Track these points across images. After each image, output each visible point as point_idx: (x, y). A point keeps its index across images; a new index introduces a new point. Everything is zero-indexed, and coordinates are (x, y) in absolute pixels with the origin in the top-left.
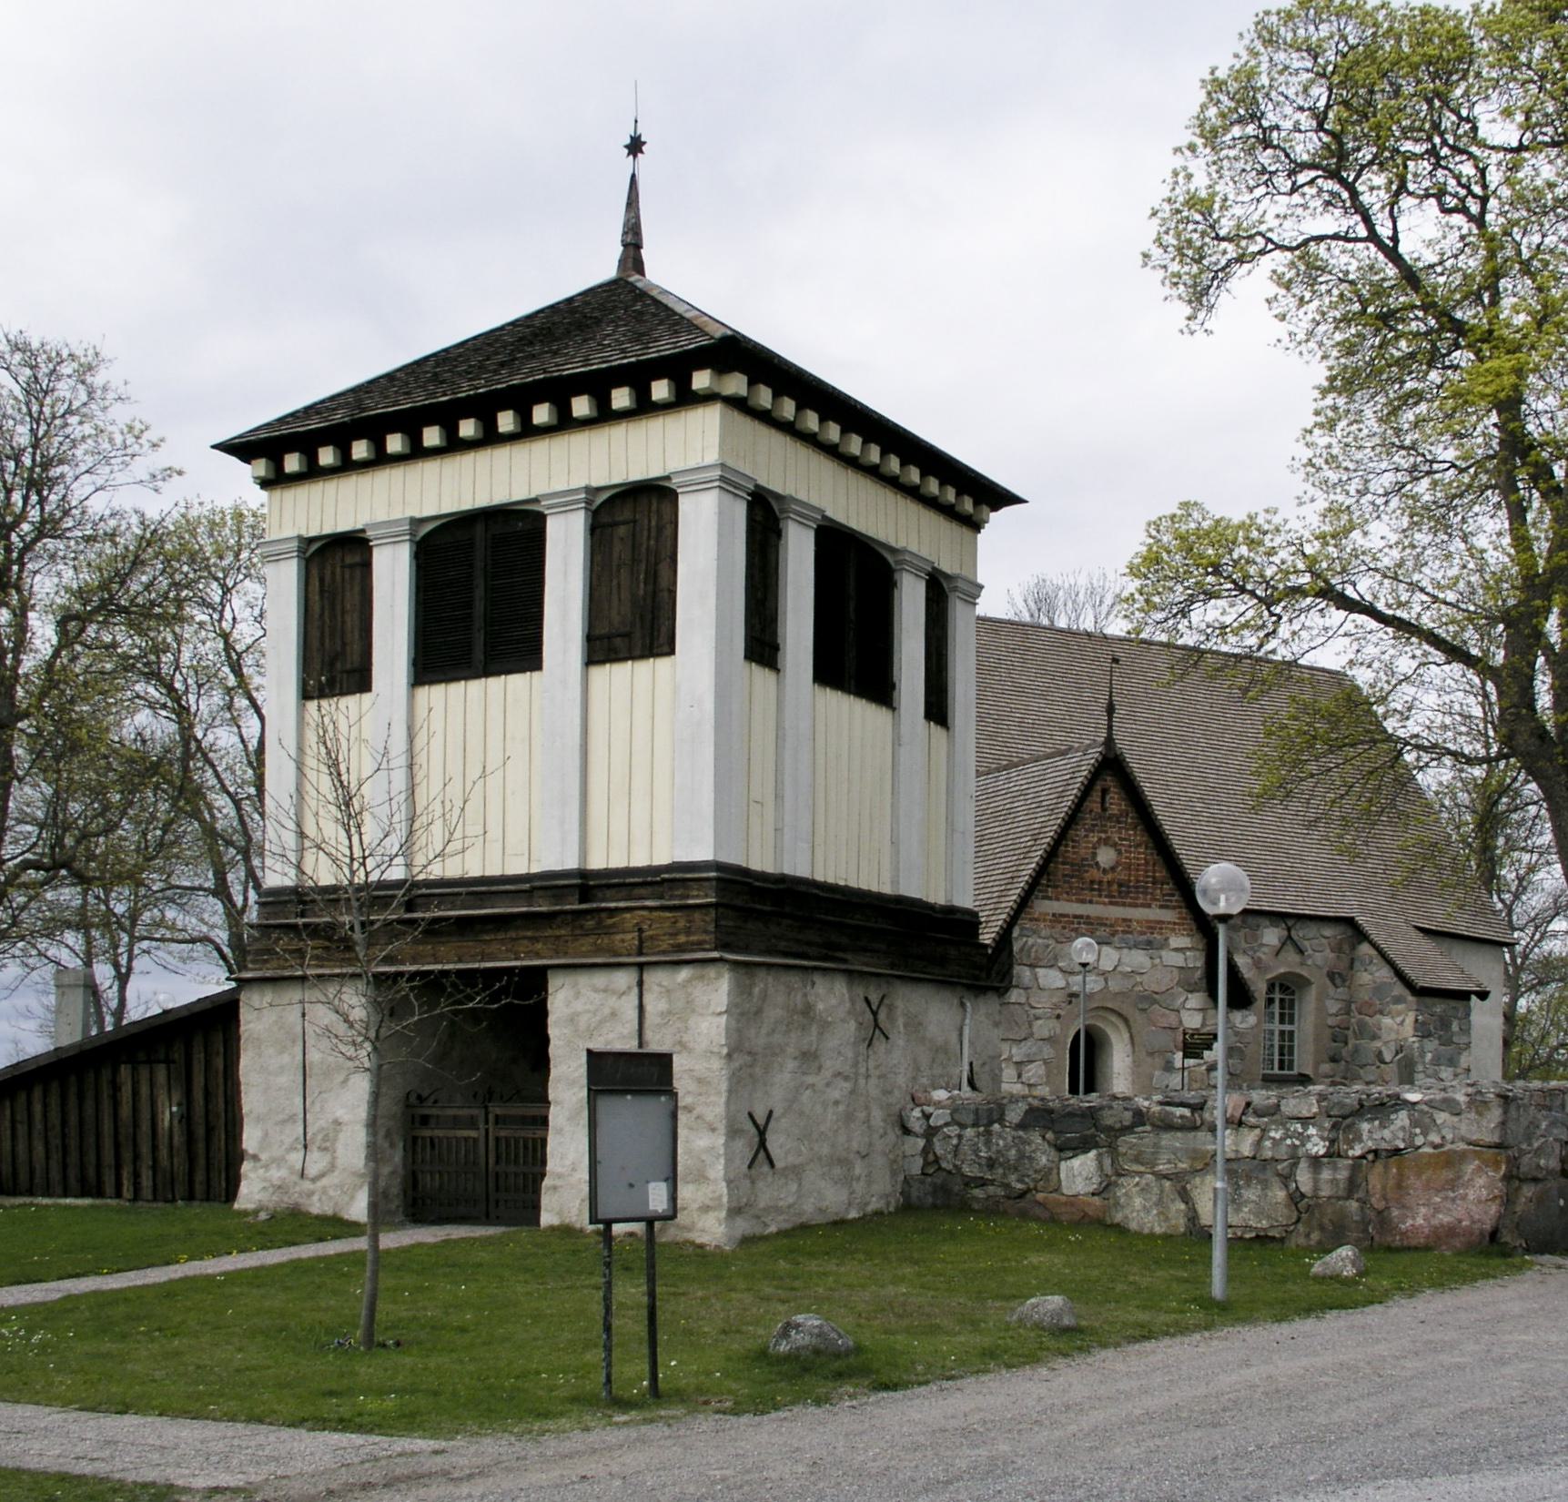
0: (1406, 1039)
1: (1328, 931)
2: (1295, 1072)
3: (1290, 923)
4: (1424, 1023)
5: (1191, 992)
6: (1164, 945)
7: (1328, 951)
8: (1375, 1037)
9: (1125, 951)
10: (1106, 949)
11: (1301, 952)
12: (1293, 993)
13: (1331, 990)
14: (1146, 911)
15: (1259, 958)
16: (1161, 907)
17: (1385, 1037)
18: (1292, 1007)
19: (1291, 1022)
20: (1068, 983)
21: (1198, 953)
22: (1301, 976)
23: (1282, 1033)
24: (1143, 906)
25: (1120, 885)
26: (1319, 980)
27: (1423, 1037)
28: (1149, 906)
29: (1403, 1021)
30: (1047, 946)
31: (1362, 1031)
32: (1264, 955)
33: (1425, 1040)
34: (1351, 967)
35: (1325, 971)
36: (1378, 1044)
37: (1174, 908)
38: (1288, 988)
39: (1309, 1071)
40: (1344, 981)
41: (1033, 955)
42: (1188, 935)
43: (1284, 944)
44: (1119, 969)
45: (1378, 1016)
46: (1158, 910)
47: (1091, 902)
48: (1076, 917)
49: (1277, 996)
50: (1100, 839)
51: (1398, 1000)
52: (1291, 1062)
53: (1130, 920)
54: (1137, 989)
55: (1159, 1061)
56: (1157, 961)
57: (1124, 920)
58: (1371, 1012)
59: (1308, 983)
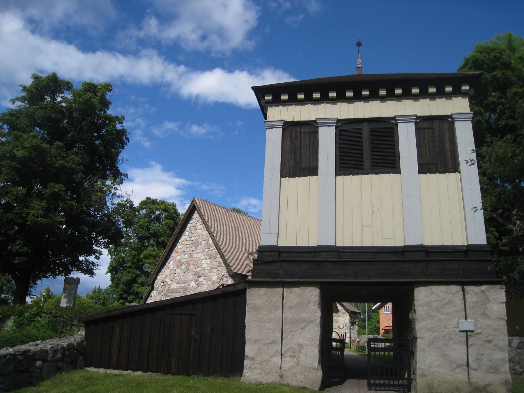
0: (347, 323)
17: (340, 322)
36: (338, 324)
51: (344, 313)
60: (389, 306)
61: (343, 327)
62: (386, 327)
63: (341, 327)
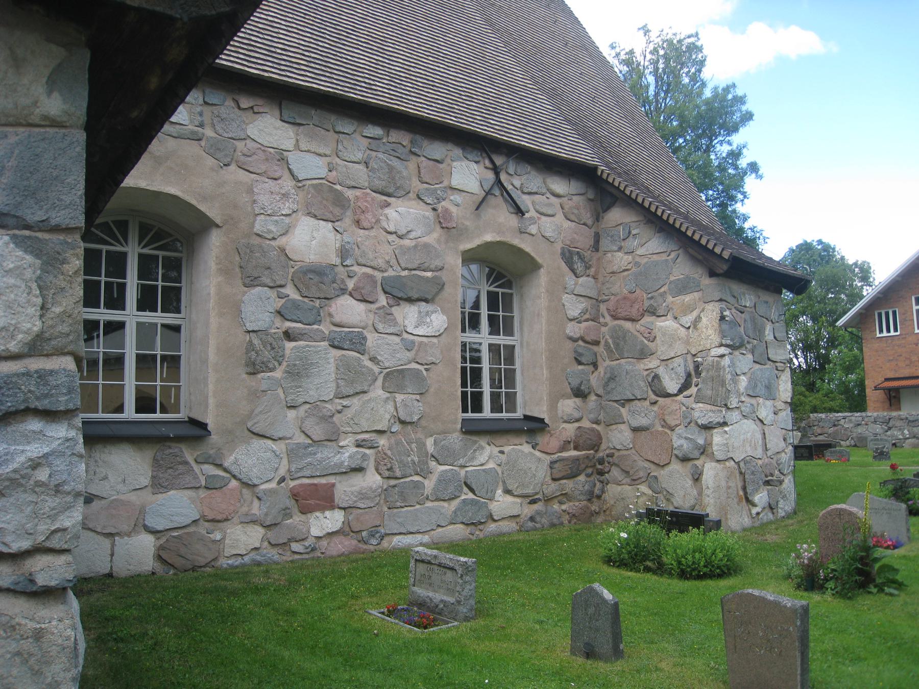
1: (559, 185)
2: (519, 414)
3: (499, 160)
4: (734, 324)
7: (560, 217)
8: (643, 354)
11: (519, 211)
12: (509, 284)
13: (570, 279)
15: (446, 210)
17: (663, 351)
18: (508, 307)
19: (509, 332)
23: (494, 349)
29: (698, 319)
32: (455, 206)
33: (737, 353)
34: (596, 247)
35: (558, 247)
36: (652, 363)
40: (588, 267)
43: (488, 193)
45: (648, 319)
51: (682, 288)
52: (511, 398)
58: (634, 313)
59: (533, 266)
60: (894, 313)
61: (685, 386)
62: (887, 380)
63: (672, 386)
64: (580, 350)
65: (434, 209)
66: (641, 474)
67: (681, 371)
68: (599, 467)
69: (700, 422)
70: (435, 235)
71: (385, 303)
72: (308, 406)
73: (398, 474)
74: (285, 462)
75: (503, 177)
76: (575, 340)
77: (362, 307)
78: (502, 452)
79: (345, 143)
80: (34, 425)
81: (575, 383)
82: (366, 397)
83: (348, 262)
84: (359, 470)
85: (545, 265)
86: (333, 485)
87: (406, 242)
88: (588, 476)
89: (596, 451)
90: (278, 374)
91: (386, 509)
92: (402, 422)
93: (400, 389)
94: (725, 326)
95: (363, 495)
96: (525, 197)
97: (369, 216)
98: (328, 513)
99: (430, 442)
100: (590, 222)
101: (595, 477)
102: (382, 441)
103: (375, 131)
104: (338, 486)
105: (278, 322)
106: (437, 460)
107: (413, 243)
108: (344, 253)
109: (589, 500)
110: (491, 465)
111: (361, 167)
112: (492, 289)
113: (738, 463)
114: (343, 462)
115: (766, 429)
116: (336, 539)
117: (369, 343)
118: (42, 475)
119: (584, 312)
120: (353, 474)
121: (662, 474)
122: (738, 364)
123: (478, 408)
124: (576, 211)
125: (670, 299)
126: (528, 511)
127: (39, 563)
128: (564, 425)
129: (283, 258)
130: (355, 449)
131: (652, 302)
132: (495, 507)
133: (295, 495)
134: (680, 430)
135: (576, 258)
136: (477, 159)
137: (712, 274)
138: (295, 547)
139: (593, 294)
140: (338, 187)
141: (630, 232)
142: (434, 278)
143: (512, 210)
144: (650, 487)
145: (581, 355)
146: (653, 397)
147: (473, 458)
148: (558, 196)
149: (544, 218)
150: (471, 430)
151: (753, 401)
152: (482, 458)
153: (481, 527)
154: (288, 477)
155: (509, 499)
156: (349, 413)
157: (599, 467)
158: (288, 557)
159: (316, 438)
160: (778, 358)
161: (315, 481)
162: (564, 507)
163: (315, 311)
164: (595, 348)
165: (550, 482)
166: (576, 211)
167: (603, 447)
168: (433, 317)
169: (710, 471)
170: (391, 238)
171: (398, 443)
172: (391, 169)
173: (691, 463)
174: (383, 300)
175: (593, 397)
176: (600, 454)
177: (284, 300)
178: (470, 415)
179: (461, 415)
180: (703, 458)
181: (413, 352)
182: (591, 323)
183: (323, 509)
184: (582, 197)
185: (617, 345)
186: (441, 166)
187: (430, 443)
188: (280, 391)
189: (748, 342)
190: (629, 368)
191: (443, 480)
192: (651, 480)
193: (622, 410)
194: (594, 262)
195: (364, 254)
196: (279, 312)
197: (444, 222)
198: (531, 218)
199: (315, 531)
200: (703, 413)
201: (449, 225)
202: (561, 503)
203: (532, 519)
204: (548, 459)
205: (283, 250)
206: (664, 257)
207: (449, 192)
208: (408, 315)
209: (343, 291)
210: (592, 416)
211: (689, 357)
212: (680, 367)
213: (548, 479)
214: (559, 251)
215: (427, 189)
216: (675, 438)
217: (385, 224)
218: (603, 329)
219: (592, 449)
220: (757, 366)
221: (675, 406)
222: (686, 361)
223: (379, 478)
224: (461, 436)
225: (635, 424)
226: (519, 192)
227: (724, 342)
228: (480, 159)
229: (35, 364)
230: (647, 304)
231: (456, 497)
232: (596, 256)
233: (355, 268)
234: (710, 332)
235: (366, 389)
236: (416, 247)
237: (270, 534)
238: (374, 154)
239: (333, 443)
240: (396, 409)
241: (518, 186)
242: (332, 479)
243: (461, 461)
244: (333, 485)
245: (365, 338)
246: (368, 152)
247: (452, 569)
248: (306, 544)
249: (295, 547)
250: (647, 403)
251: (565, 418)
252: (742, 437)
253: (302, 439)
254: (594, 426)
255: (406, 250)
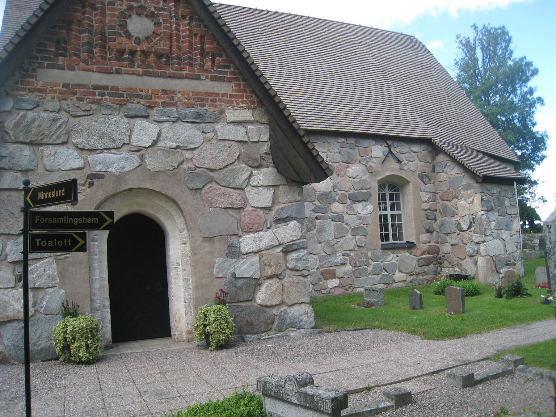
3: (390, 143)
4: (487, 201)
5: (257, 167)
6: (218, 118)
7: (417, 161)
8: (454, 214)
9: (166, 125)
10: (138, 121)
11: (399, 162)
12: (397, 190)
13: (422, 186)
14: (195, 83)
15: (370, 166)
16: (213, 79)
17: (461, 213)
19: (399, 209)
20: (86, 162)
21: (262, 127)
22: (401, 177)
24: (187, 77)
25: (159, 56)
26: (414, 180)
27: (488, 211)
28: (198, 78)
29: (473, 200)
30: (55, 120)
31: (445, 212)
32: (373, 164)
33: (490, 213)
34: (433, 171)
35: (417, 173)
36: (457, 218)
37: (229, 80)
38: (394, 187)
39: (413, 240)
40: (430, 180)
41: (34, 131)
42: (249, 108)
43: (387, 156)
44: (160, 144)
45: (455, 200)
46: (209, 83)
47: (118, 72)
48: (96, 87)
49: (387, 192)
50: (130, 8)
51: (467, 188)
52: (401, 235)
53: (174, 92)
54: (184, 166)
55: (219, 246)
56: (210, 135)
57: (165, 92)
58: (449, 198)
59: (407, 182)
61: (470, 227)
63: (465, 227)
64: (428, 214)
65: (366, 166)
66: (455, 263)
67: (468, 221)
68: (439, 261)
69: (475, 241)
70: (367, 176)
71: (350, 203)
72: (325, 242)
73: (358, 265)
74: (318, 262)
75: (392, 149)
76: (426, 210)
77: (342, 205)
78: (397, 256)
79: (332, 146)
80: (302, 250)
81: (427, 227)
82: (345, 238)
83: (336, 190)
84: (344, 264)
85: (411, 181)
86: (335, 270)
87: (356, 180)
88: (435, 265)
89: (438, 255)
90: (314, 232)
91: (354, 278)
92: (359, 246)
93: (357, 234)
94: (484, 203)
95: (346, 273)
96: (401, 155)
97: (342, 172)
98: (334, 280)
99: (369, 253)
100: (430, 161)
101: (438, 265)
102: (352, 254)
103: (342, 140)
104: (337, 270)
105: (313, 213)
106: (372, 260)
107: (359, 180)
108: (334, 187)
109: (435, 274)
110: (393, 261)
111: (338, 154)
112: (391, 192)
113: (492, 257)
114: (338, 261)
115: (506, 243)
116: (337, 289)
117: (345, 218)
118: (304, 258)
119: (429, 198)
120: (342, 266)
121: (463, 262)
122: (490, 217)
123: (387, 239)
124: (424, 158)
125: (463, 192)
126: (409, 279)
127: (304, 271)
128: (423, 245)
129: (313, 191)
130: (342, 257)
131: (456, 193)
132: (395, 277)
133: (322, 274)
134: (468, 245)
135: (425, 177)
136: (381, 144)
137: (477, 183)
138: (323, 291)
139: (433, 190)
140: (330, 163)
141: (446, 165)
142: (368, 192)
143: (396, 161)
144: (459, 268)
145: (429, 216)
146: (458, 232)
147: (386, 259)
148: (416, 152)
149: (410, 163)
150: (385, 248)
151: (499, 232)
152: (390, 258)
153: (390, 285)
154: (320, 267)
155: (401, 274)
156: (339, 244)
157: (439, 261)
158: (321, 295)
159: (328, 253)
160: (512, 213)
161: (329, 268)
162: (424, 277)
163: (325, 209)
164: (435, 213)
165: (418, 267)
166: (424, 158)
167: (440, 252)
168: (368, 206)
169: (481, 261)
170: (350, 179)
171: (357, 254)
172: (349, 153)
173: (473, 258)
174: (349, 202)
175: (435, 233)
176: (439, 256)
177: (314, 206)
178: (384, 242)
179: (380, 243)
180: (477, 255)
181: (361, 220)
182: (432, 203)
183: (332, 278)
184: (426, 151)
185: (444, 211)
186: (367, 149)
187: (369, 254)
188: (315, 238)
189: (496, 208)
190: (449, 220)
191: (375, 267)
192: (459, 265)
193: (447, 237)
194: (432, 178)
195: (341, 186)
196: (313, 210)
197: (371, 171)
198: (405, 163)
199: (330, 286)
200: (476, 237)
201: (372, 171)
202: (423, 276)
203: (411, 282)
204: (417, 258)
205: (313, 188)
206: (460, 175)
207: (371, 158)
208: (359, 207)
209: (335, 200)
210: (435, 240)
211: (471, 216)
212: (467, 219)
213: (417, 266)
214: (417, 175)
215: (363, 159)
216: (467, 248)
217: (348, 174)
218: (438, 205)
219: (436, 254)
220: (501, 217)
221: (466, 235)
222: (469, 217)
223: (351, 267)
224: (381, 251)
225: (452, 243)
226: (399, 154)
227: (483, 209)
228: (383, 143)
229: (301, 241)
230: (454, 194)
231: (380, 274)
232: (433, 174)
233: (339, 192)
234: (478, 205)
235: (345, 235)
236: (360, 181)
237: (314, 287)
238: (342, 149)
239: (334, 255)
240: (356, 241)
241: (398, 152)
242: (335, 268)
243: (381, 260)
244: (335, 270)
245: (343, 217)
246: (340, 148)
247: (377, 291)
248: (327, 290)
249: (323, 291)
250: (456, 234)
251: (423, 242)
252: (493, 247)
253: (324, 254)
254: (436, 244)
255: (356, 183)
